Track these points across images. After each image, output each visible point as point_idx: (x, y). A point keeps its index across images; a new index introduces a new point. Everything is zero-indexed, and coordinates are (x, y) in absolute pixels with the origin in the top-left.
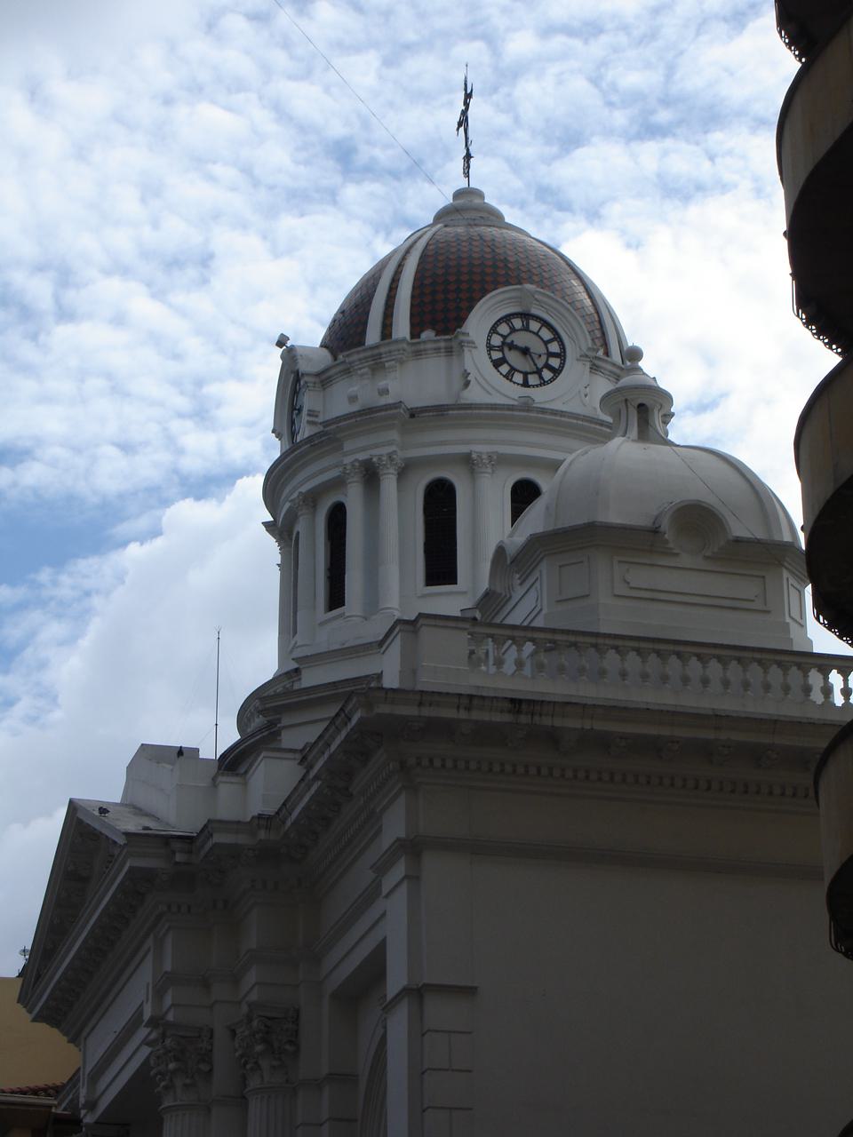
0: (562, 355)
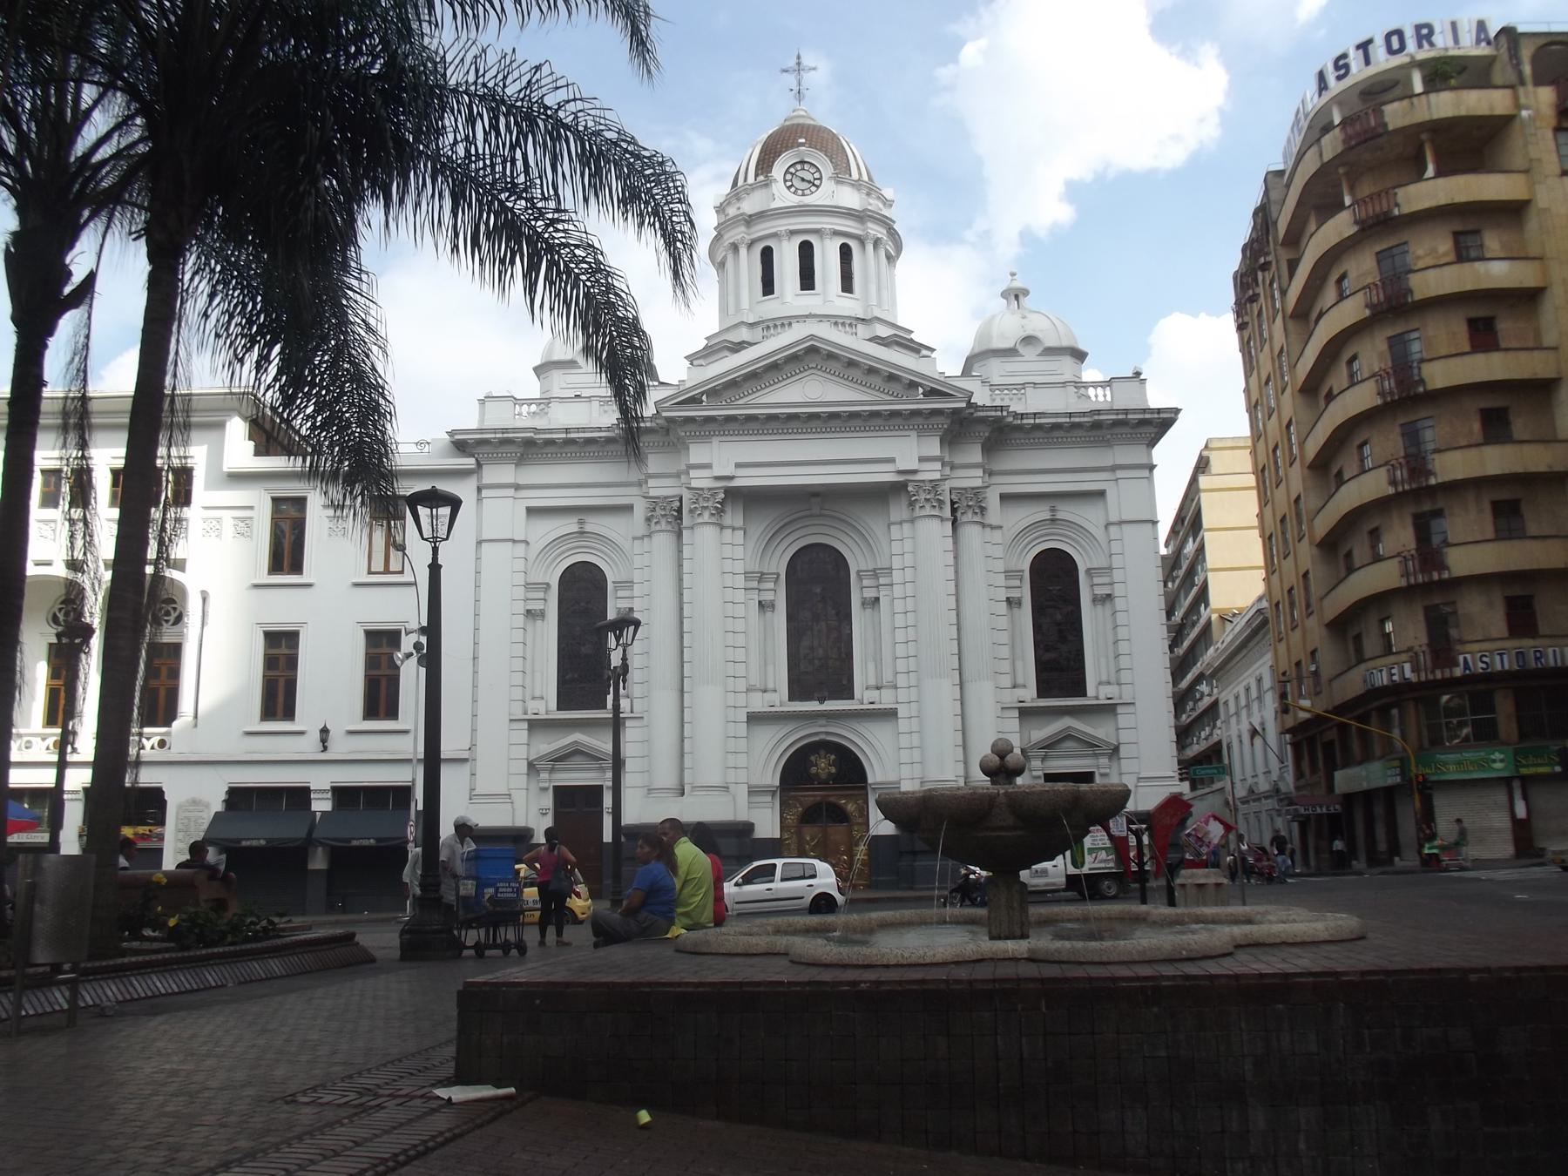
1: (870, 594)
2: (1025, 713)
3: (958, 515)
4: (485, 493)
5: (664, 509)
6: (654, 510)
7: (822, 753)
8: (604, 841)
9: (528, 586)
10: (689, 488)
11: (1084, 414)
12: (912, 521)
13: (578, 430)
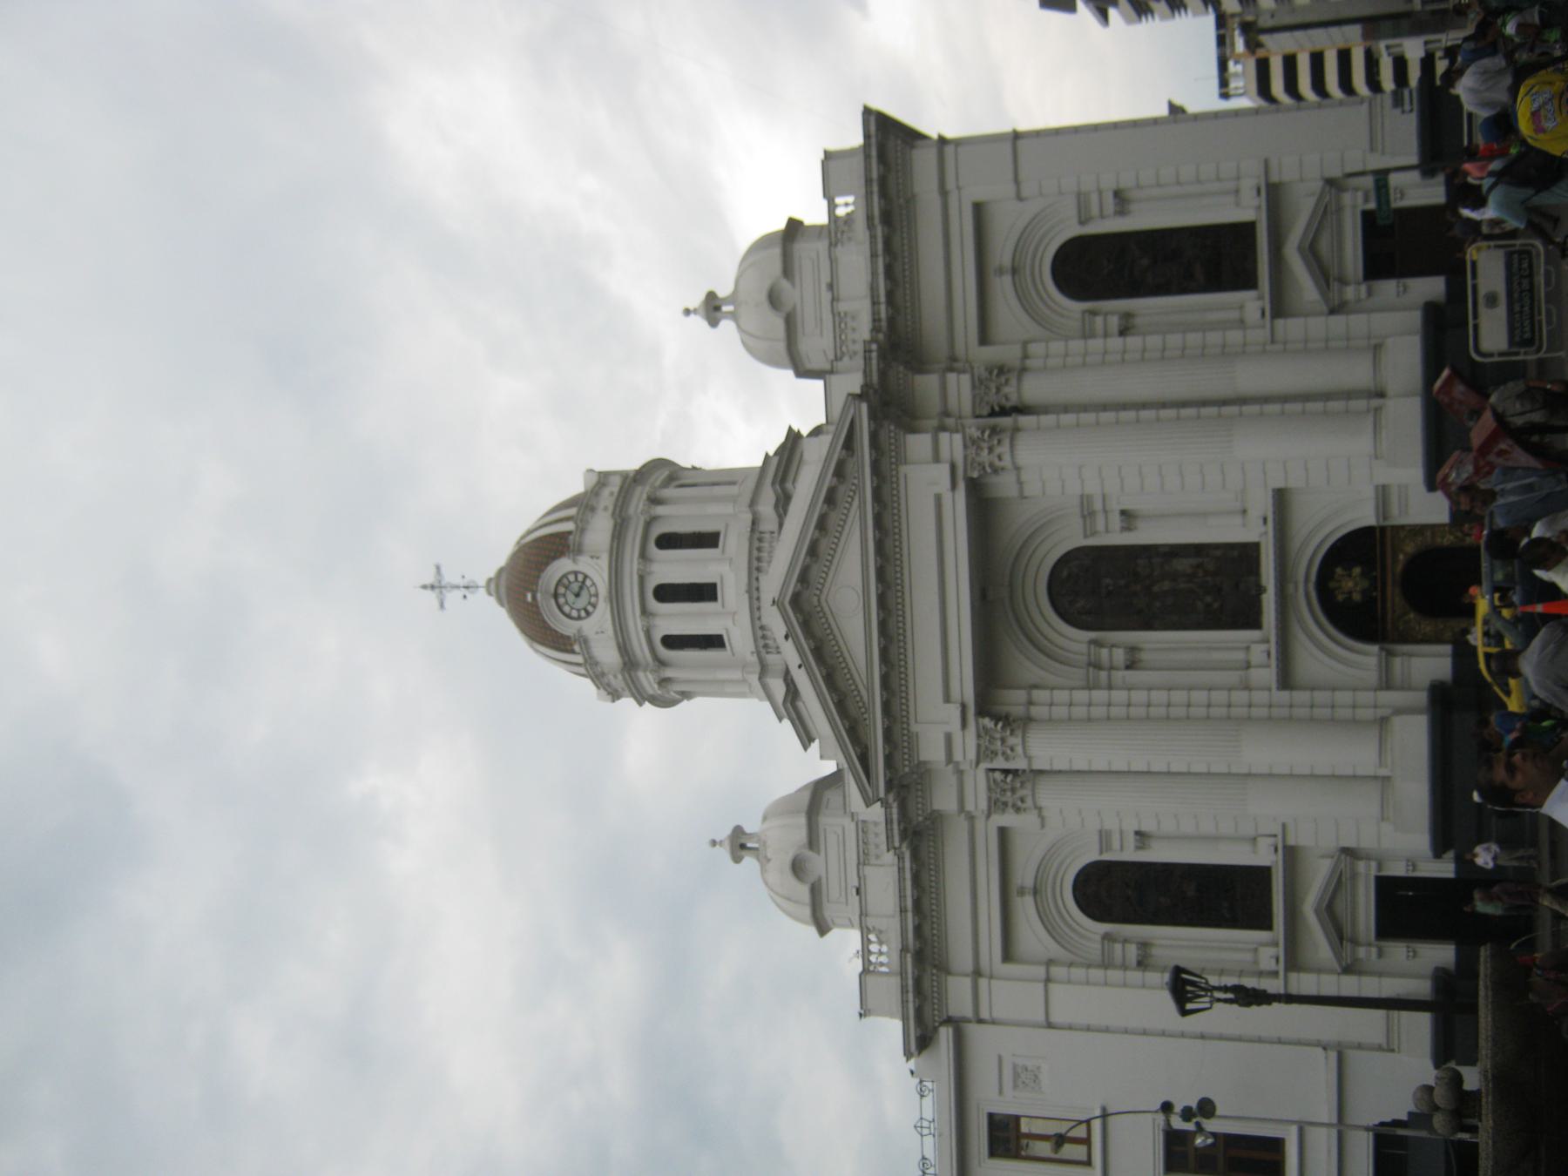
0: (576, 573)
1: (1116, 521)
2: (1279, 308)
3: (1008, 405)
4: (985, 1014)
5: (1004, 790)
6: (1005, 804)
7: (1332, 585)
8: (1451, 875)
9: (1106, 964)
10: (978, 763)
11: (873, 238)
12: (1017, 469)
13: (902, 897)
